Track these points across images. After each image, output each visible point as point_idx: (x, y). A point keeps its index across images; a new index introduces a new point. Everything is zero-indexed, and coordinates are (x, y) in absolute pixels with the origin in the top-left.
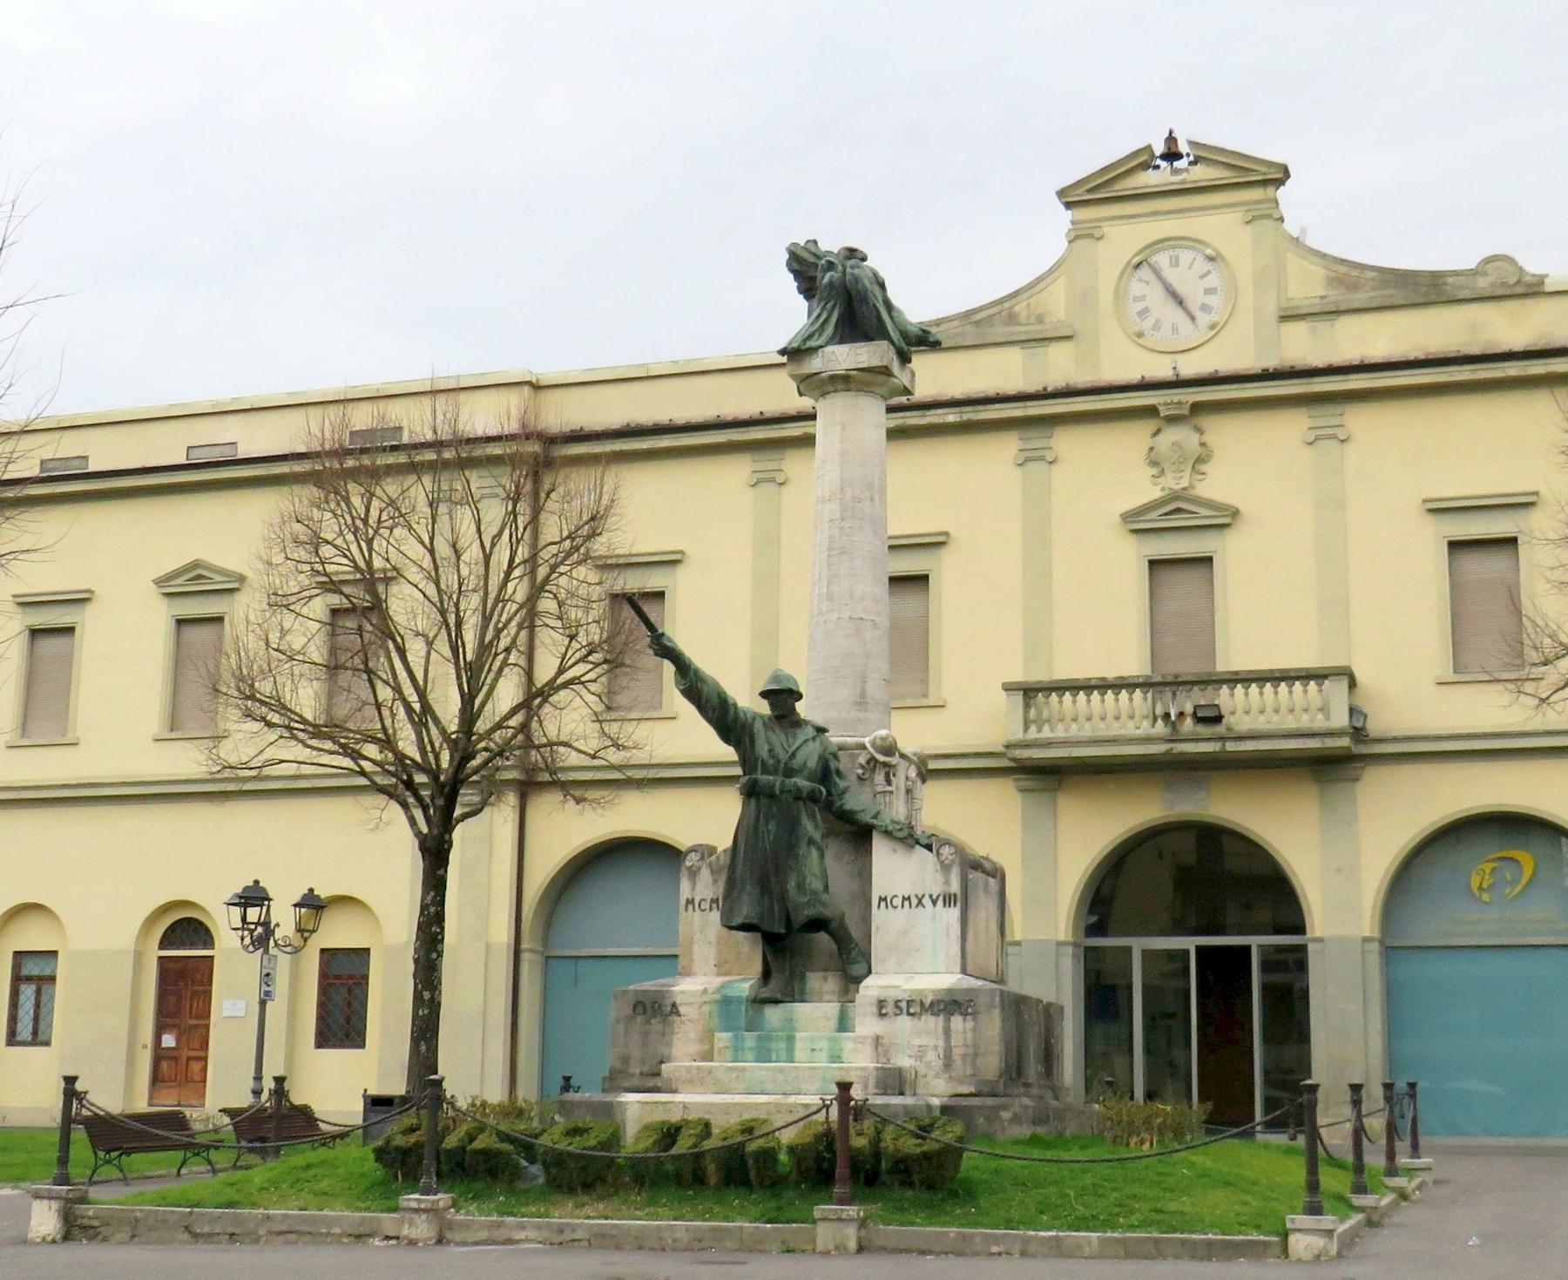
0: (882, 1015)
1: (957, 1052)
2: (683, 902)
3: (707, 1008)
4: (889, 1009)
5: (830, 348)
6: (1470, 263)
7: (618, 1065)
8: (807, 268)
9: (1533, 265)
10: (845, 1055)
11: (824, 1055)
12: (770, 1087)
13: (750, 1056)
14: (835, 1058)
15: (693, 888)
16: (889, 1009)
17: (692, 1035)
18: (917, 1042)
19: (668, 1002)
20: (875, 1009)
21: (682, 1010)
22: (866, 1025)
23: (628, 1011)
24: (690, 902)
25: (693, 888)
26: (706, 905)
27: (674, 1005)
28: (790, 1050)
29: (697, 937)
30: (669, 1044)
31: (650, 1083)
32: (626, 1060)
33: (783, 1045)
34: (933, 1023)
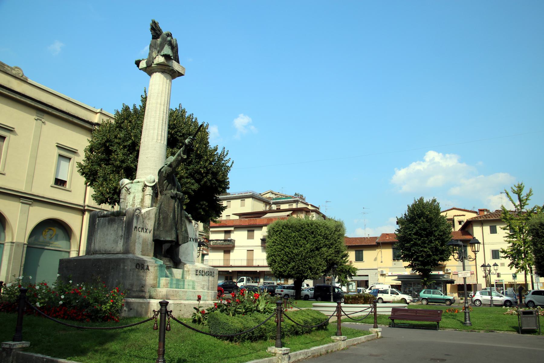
0: (197, 275)
1: (210, 286)
2: (134, 227)
3: (156, 268)
4: (198, 273)
5: (174, 61)
6: (13, 66)
7: (130, 287)
8: (156, 31)
9: (26, 75)
10: (196, 287)
11: (191, 287)
12: (192, 298)
13: (174, 286)
14: (193, 288)
15: (137, 223)
16: (198, 273)
17: (152, 277)
18: (203, 283)
19: (146, 265)
20: (195, 272)
21: (150, 268)
22: (190, 277)
23: (134, 267)
24: (136, 227)
25: (137, 223)
26: (140, 230)
27: (148, 266)
28: (184, 285)
29: (137, 240)
30: (145, 280)
31: (141, 294)
32: (132, 285)
33: (182, 283)
34: (206, 278)
